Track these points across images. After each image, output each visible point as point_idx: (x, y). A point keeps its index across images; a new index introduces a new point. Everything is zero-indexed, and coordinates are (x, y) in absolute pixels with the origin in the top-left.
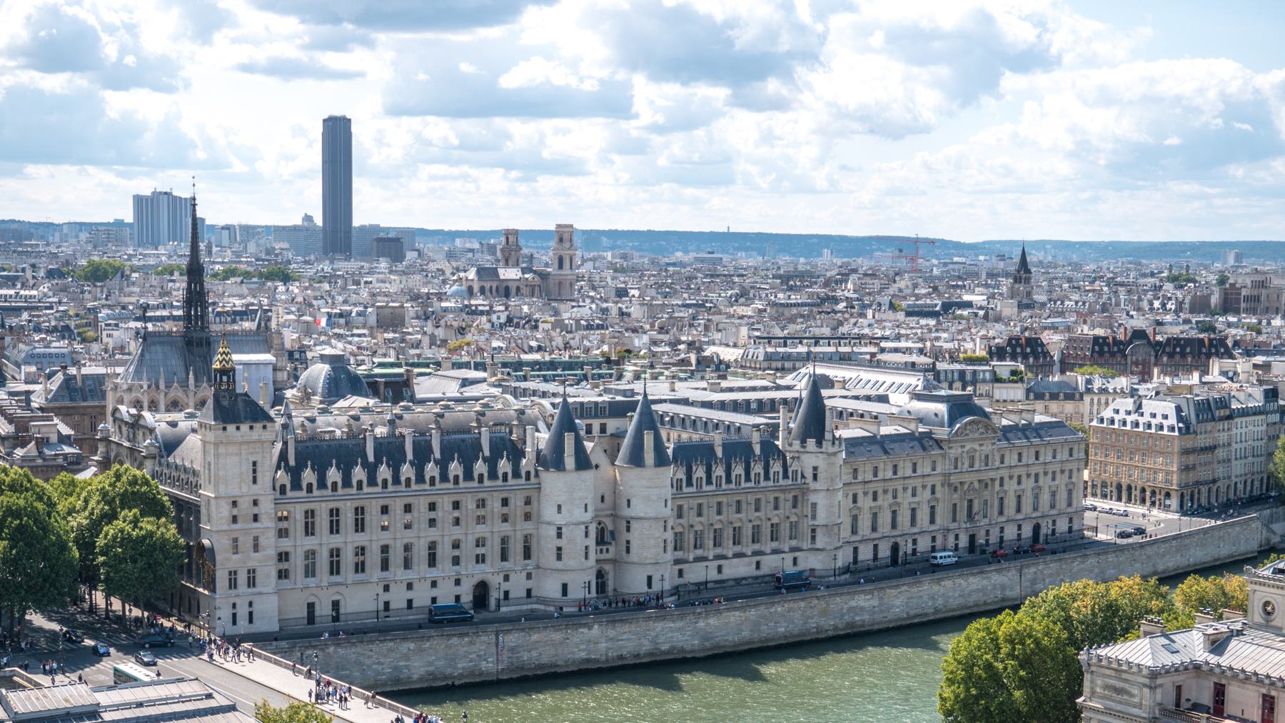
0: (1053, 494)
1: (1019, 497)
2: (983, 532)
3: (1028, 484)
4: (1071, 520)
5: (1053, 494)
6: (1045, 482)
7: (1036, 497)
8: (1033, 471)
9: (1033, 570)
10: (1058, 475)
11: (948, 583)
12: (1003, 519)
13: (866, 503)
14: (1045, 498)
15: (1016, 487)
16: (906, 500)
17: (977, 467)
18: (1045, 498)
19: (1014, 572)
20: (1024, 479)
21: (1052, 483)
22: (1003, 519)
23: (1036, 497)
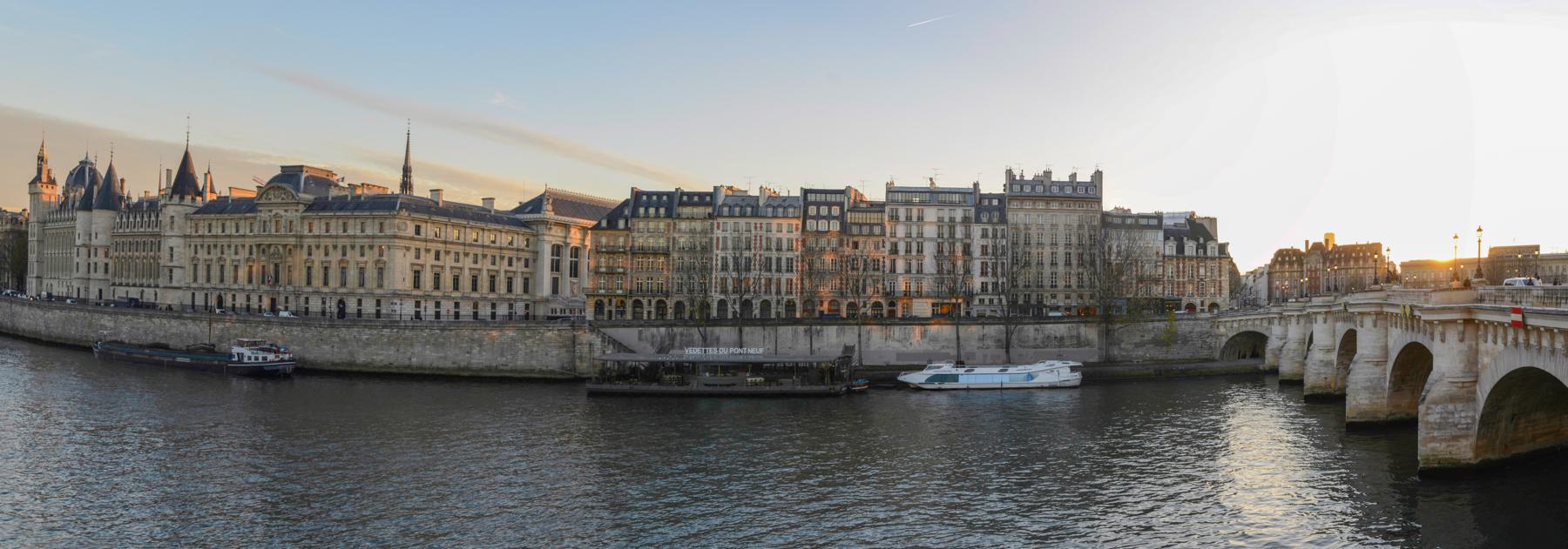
0: (362, 271)
1: (326, 269)
2: (282, 298)
3: (335, 257)
4: (378, 303)
5: (362, 271)
6: (353, 257)
7: (343, 271)
8: (341, 242)
9: (221, 326)
10: (367, 251)
11: (157, 321)
12: (310, 289)
13: (202, 255)
14: (352, 274)
15: (323, 258)
16: (229, 257)
17: (282, 231)
18: (352, 274)
19: (205, 324)
20: (331, 250)
21: (360, 259)
22: (310, 289)
23: (343, 271)
